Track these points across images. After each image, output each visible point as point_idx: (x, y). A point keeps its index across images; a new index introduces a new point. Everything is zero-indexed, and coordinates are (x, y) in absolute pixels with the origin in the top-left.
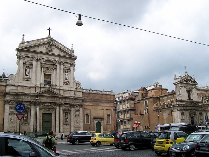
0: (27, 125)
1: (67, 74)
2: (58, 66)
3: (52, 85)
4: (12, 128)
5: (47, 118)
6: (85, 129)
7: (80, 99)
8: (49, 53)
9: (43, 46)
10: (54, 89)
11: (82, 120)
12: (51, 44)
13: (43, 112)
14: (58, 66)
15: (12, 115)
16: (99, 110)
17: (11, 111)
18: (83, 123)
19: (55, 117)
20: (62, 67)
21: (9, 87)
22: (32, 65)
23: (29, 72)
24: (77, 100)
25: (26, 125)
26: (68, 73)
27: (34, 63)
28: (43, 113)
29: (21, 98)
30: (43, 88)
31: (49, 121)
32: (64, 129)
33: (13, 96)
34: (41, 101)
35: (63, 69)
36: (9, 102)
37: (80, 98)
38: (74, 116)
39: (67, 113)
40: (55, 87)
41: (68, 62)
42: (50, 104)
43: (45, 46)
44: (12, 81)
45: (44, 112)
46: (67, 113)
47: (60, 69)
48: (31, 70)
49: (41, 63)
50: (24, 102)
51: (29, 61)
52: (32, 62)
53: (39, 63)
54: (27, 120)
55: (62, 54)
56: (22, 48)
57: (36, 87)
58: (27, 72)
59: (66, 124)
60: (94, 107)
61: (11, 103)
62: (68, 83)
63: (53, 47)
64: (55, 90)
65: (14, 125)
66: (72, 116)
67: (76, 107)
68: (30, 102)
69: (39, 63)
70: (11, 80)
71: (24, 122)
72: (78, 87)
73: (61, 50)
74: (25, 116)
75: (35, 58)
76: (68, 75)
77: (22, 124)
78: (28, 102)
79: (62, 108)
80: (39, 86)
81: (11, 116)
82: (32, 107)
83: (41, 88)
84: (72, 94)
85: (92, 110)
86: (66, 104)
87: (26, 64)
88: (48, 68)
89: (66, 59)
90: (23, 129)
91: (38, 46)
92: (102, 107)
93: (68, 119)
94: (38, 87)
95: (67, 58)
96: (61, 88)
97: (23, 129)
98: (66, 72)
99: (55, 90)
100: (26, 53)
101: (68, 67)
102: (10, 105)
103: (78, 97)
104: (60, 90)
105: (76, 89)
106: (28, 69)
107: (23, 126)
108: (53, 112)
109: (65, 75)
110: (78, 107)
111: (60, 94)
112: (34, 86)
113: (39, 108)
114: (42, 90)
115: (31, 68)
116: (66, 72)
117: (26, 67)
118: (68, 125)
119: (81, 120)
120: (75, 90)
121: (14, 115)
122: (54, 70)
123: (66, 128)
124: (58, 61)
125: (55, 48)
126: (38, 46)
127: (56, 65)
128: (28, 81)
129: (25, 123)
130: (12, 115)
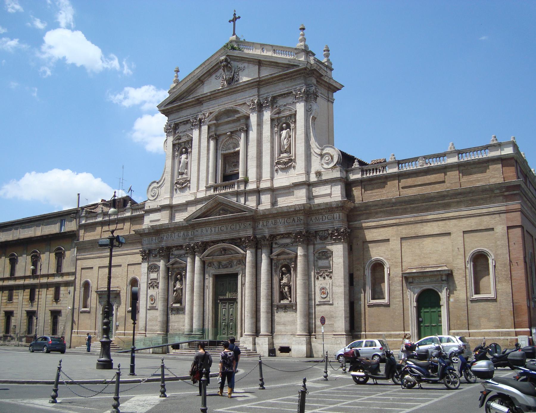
7: (329, 209)
9: (214, 76)
12: (226, 60)
15: (154, 288)
16: (428, 241)
17: (151, 278)
23: (187, 163)
24: (321, 214)
29: (165, 238)
32: (279, 324)
33: (154, 238)
34: (205, 239)
41: (285, 91)
42: (225, 245)
43: (218, 74)
44: (155, 198)
47: (260, 124)
48: (189, 157)
50: (175, 249)
52: (191, 132)
53: (205, 128)
54: (179, 300)
55: (266, 73)
56: (165, 106)
57: (196, 202)
60: (405, 231)
63: (234, 64)
67: (321, 239)
70: (153, 196)
72: (326, 166)
73: (260, 63)
76: (290, 137)
85: (395, 243)
86: (280, 238)
87: (179, 144)
89: (281, 84)
90: (173, 324)
91: (201, 81)
92: (440, 223)
93: (290, 288)
95: (281, 79)
97: (173, 324)
100: (177, 113)
120: (313, 178)
123: (283, 320)
125: (246, 65)
126: (201, 81)
130: (154, 288)
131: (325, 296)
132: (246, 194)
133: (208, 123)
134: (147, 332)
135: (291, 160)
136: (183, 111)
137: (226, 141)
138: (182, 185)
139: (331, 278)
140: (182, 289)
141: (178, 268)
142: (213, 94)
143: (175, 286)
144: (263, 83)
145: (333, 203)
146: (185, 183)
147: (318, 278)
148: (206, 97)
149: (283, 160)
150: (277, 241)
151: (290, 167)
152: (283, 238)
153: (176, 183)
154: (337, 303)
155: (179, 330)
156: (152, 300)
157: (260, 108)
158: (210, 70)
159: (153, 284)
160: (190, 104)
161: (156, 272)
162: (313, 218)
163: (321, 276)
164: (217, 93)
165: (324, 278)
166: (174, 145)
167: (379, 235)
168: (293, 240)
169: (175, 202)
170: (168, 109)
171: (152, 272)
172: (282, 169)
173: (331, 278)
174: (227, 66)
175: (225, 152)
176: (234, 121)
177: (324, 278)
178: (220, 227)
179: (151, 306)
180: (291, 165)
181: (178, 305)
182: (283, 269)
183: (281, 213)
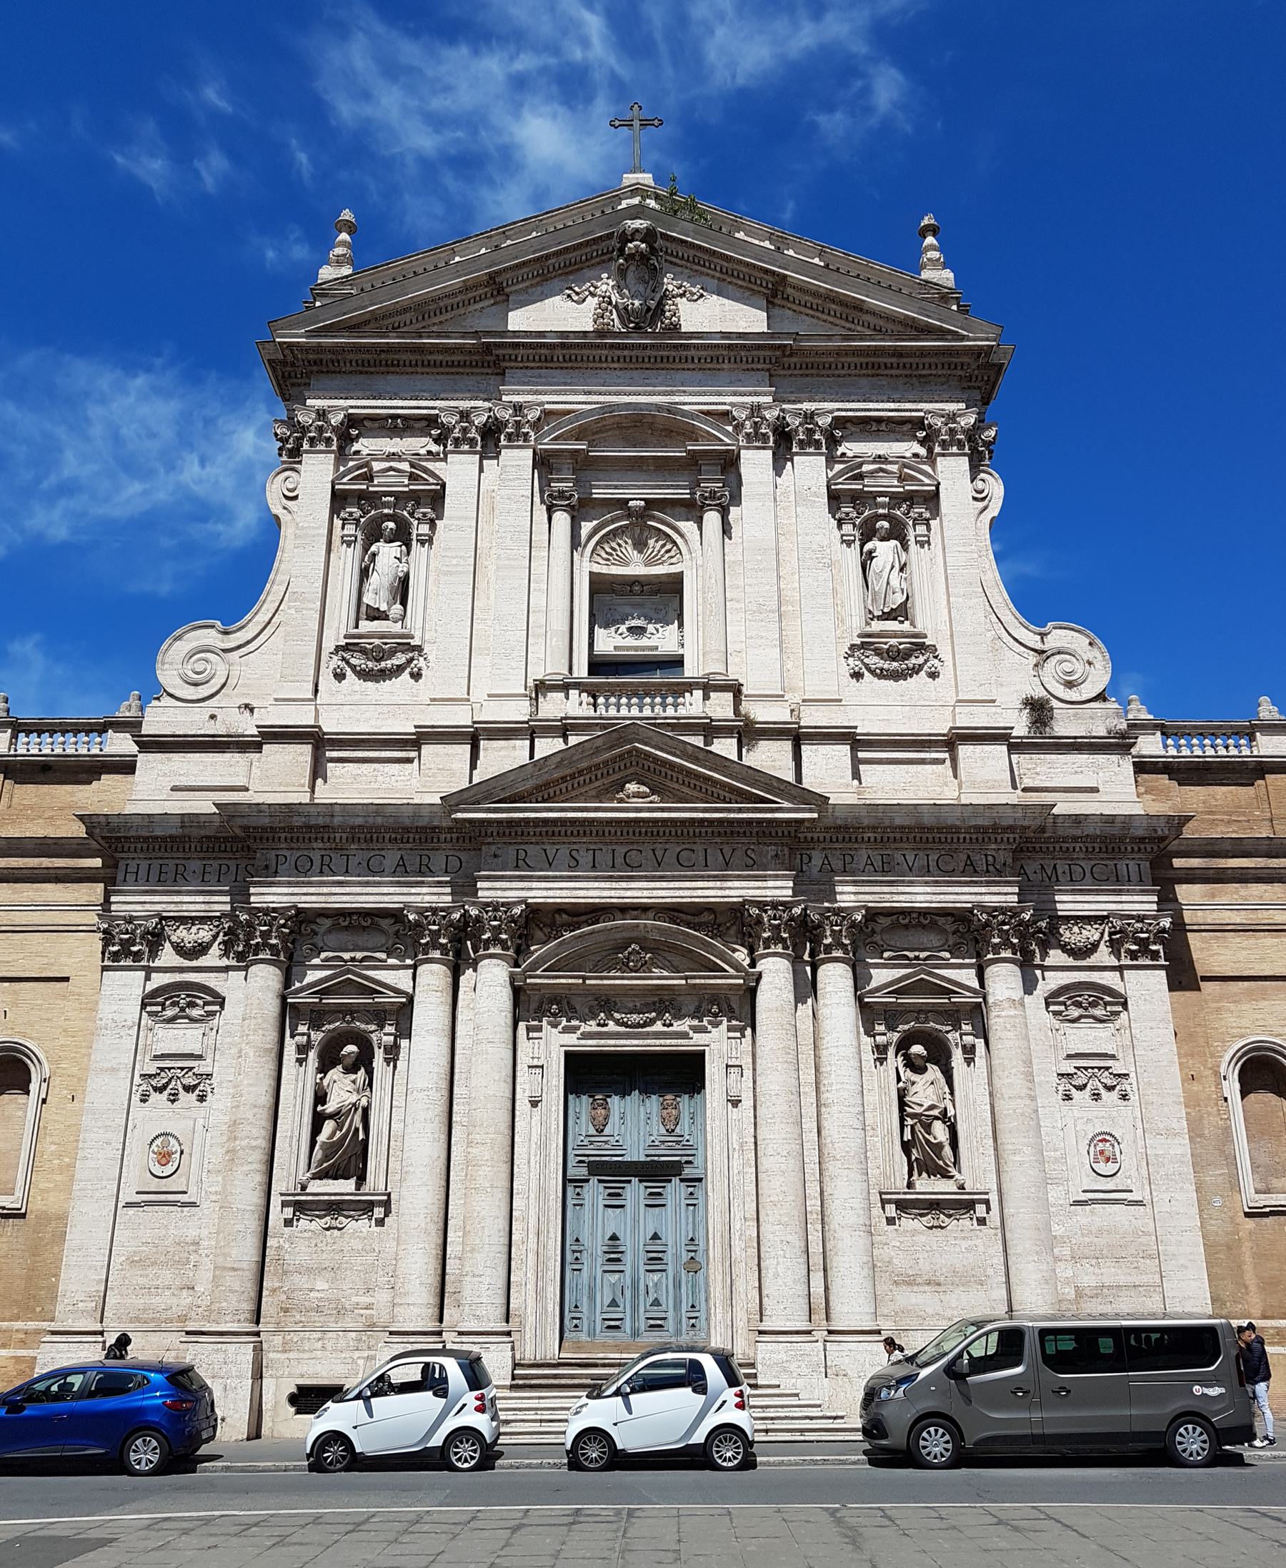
0: (361, 1227)
1: (885, 550)
2: (755, 464)
3: (689, 687)
4: (166, 1276)
5: (634, 1124)
6: (1250, 1277)
8: (645, 342)
10: (710, 730)
11: (1181, 1147)
12: (649, 236)
13: (572, 1040)
14: (755, 464)
15: (174, 1098)
18: (1203, 1204)
19: (747, 1103)
20: (810, 471)
21: (166, 768)
22: (437, 499)
25: (352, 1225)
26: (897, 533)
27: (458, 471)
28: (573, 1060)
30: (564, 728)
31: (657, 1172)
35: (835, 498)
36: (155, 939)
37: (1111, 819)
38: (1030, 1077)
39: (924, 1032)
40: (720, 707)
45: (591, 1045)
46: (924, 1032)
49: (543, 463)
50: (328, 923)
51: (405, 466)
53: (517, 461)
54: (348, 1158)
56: (310, 334)
57: (474, 737)
58: (374, 579)
59: (934, 1206)
61: (167, 956)
62: (906, 655)
64: (725, 747)
65: (192, 1233)
66: (1010, 1081)
68: (396, 915)
69: (517, 461)
71: (316, 1187)
74: (330, 1107)
75: (465, 415)
77: (289, 1212)
78: (385, 923)
79: (835, 979)
80: (518, 712)
81: (157, 1115)
82: (433, 976)
83: (531, 732)
84: (984, 780)
86: (895, 926)
88: (630, 513)
90: (300, 1281)
94: (505, 732)
96: (812, 718)
97: (300, 1281)
98: (868, 532)
99: (725, 747)
101: (894, 468)
102: (159, 980)
103: (1078, 819)
104: (797, 737)
105: (1039, 710)
106: (387, 553)
107: (301, 1242)
108: (716, 1042)
109: (867, 559)
110: (1103, 956)
111: (796, 792)
112: (460, 717)
113: (518, 993)
114: (547, 747)
115: (424, 529)
116: (868, 532)
117: (373, 534)
118: (966, 1223)
119: (1158, 1146)
120: (1021, 726)
121: (202, 1098)
122: (712, 519)
124: (756, 410)
127: (729, 463)
128: (386, 685)
129: (334, 1207)
131: (1110, 1168)
132: (748, 733)
133: (547, 445)
134: (261, 1327)
135: (922, 648)
136: (389, 377)
137: (614, 534)
138: (378, 660)
139: (1124, 1097)
140: (366, 1111)
141: (350, 1011)
142: (571, 346)
143: (320, 1097)
144: (794, 360)
145: (1137, 823)
146: (392, 653)
147: (1068, 1097)
148: (530, 345)
149: (893, 641)
150: (877, 938)
151: (916, 670)
152: (906, 927)
153: (346, 648)
154: (1166, 1197)
155: (341, 1312)
156: (164, 1158)
157: (784, 444)
158: (547, 257)
159: (176, 1079)
160: (439, 357)
161: (193, 1020)
162: (1032, 867)
163: (1081, 1088)
164: (591, 346)
165: (1096, 1096)
166: (339, 499)
167: (1262, 960)
168: (950, 943)
169: (331, 724)
170: (319, 349)
171: (172, 1020)
172: (882, 675)
173: (1124, 1097)
174: (643, 258)
175: (605, 570)
176: (663, 467)
177: (1096, 1096)
178: (623, 850)
179: (154, 1185)
180: (921, 666)
181: (345, 1187)
182: (917, 1049)
183: (930, 829)
